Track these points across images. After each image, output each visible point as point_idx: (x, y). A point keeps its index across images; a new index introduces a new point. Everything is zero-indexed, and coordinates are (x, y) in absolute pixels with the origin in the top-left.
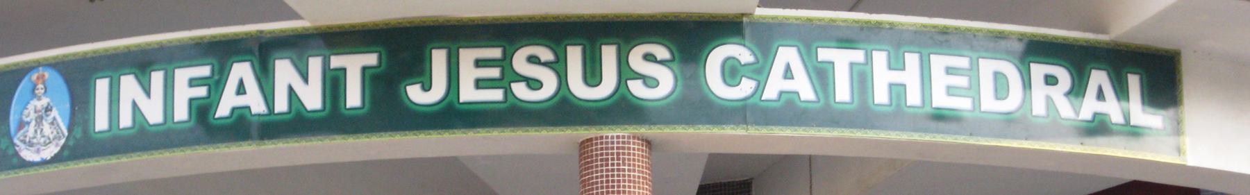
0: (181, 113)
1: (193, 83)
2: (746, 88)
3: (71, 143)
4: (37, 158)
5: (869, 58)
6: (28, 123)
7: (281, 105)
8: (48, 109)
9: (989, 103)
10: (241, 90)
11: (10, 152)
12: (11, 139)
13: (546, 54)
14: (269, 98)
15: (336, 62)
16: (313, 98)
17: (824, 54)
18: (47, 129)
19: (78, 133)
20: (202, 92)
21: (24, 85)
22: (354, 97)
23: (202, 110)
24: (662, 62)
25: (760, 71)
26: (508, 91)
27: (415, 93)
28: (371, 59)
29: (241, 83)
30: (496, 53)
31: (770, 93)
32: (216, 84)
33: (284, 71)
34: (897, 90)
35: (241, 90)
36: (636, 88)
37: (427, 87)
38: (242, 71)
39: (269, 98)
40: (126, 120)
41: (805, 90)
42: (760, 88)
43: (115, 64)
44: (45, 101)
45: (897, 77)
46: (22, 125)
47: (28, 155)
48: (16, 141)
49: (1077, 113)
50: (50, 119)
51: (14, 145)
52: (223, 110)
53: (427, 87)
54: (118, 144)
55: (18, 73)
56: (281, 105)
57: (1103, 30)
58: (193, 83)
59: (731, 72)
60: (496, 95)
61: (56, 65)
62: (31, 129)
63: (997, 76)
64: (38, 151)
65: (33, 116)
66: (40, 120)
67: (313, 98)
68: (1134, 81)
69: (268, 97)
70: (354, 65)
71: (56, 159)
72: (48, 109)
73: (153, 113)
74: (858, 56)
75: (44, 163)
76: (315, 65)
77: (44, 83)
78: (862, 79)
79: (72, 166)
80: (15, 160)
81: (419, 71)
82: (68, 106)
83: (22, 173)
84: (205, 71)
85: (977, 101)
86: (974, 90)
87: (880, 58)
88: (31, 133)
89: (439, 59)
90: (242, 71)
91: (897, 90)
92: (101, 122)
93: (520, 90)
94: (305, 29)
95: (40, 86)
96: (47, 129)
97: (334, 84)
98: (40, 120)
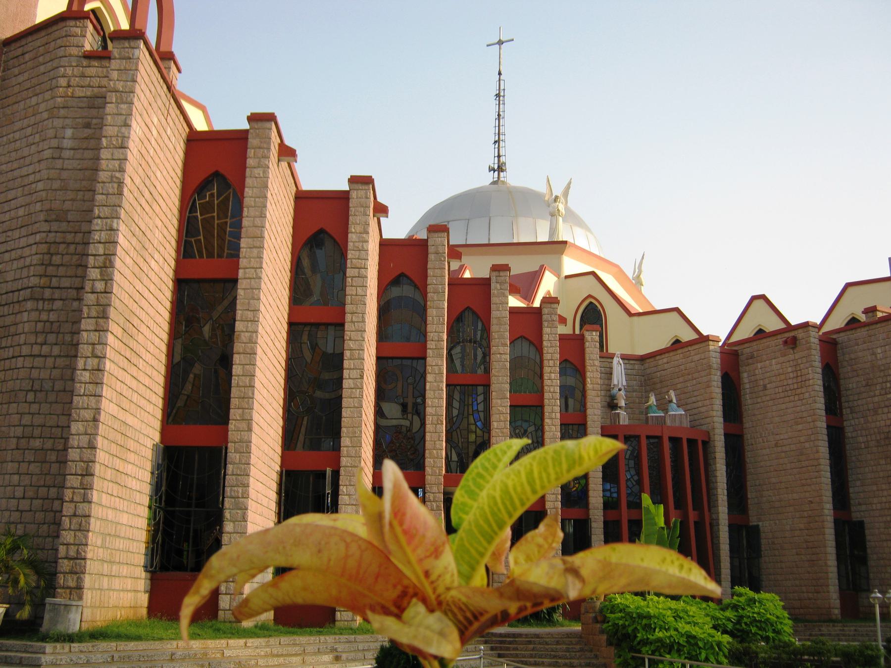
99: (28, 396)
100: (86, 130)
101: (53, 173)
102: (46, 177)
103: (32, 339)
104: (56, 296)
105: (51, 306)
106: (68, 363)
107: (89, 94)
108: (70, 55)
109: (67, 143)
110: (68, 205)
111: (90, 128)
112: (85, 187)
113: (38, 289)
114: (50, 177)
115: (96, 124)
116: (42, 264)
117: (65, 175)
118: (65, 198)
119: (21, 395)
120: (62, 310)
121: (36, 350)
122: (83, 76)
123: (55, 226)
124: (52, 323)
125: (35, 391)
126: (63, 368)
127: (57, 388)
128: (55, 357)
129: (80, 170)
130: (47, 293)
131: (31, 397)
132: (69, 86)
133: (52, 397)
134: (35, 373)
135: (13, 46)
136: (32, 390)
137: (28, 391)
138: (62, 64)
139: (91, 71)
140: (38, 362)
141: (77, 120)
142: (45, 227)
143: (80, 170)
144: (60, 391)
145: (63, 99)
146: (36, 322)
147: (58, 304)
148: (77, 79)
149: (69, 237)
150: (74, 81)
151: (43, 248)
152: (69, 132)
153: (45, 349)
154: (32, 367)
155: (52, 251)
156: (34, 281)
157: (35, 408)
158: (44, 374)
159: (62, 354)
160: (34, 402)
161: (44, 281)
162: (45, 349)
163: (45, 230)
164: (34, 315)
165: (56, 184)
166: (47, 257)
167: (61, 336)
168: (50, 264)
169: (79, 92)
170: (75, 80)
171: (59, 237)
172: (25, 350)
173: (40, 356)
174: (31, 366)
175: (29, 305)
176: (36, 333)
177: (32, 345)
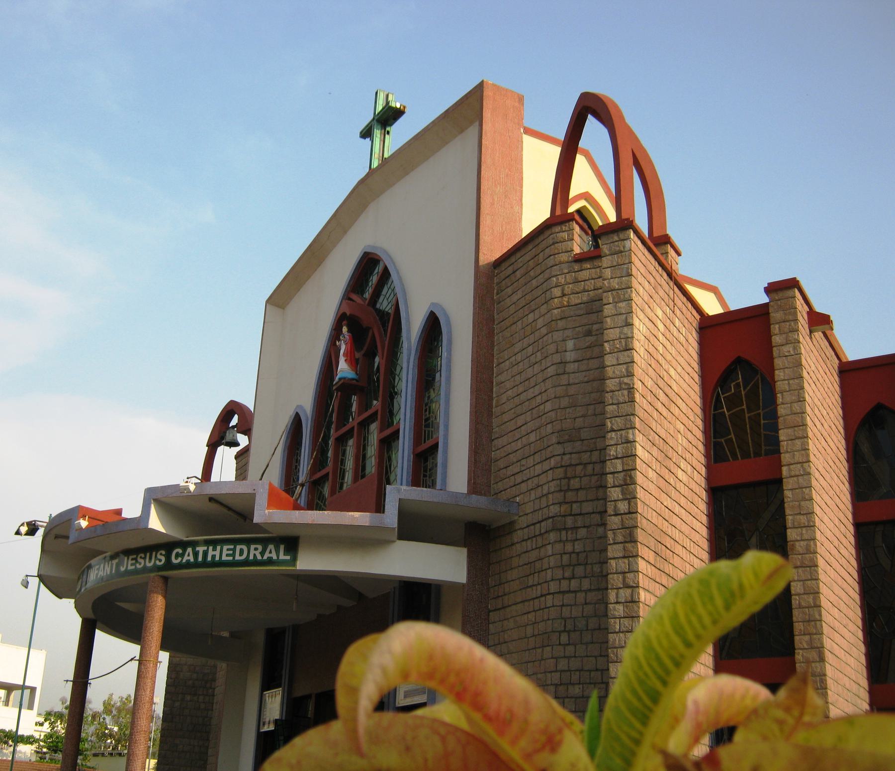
2: (180, 559)
5: (208, 548)
9: (238, 557)
25: (183, 555)
31: (184, 561)
34: (214, 556)
42: (182, 560)
45: (214, 553)
49: (263, 558)
59: (177, 555)
68: (282, 547)
74: (205, 548)
78: (205, 554)
85: (234, 557)
86: (233, 555)
87: (211, 548)
91: (214, 556)
99: (562, 638)
100: (588, 339)
101: (560, 391)
102: (553, 396)
103: (559, 573)
104: (579, 524)
105: (574, 535)
106: (600, 597)
107: (585, 299)
108: (561, 263)
109: (570, 356)
110: (579, 423)
111: (592, 336)
113: (560, 518)
114: (557, 396)
116: (561, 491)
117: (572, 390)
118: (575, 416)
121: (565, 585)
122: (576, 281)
123: (569, 447)
124: (578, 554)
125: (569, 632)
126: (595, 604)
127: (591, 626)
128: (586, 591)
129: (587, 382)
130: (569, 521)
131: (564, 638)
132: (564, 295)
133: (587, 637)
134: (566, 612)
135: (503, 266)
136: (564, 631)
137: (560, 632)
138: (554, 273)
139: (585, 274)
140: (569, 598)
141: (577, 329)
142: (559, 449)
143: (587, 382)
144: (595, 629)
145: (559, 310)
146: (561, 554)
147: (582, 532)
148: (571, 286)
149: (585, 457)
150: (567, 289)
151: (560, 472)
153: (574, 584)
154: (563, 605)
155: (569, 475)
156: (554, 510)
157: (570, 650)
158: (576, 612)
159: (593, 587)
160: (569, 644)
161: (564, 508)
162: (574, 584)
163: (559, 453)
164: (559, 547)
165: (565, 402)
166: (564, 482)
167: (589, 567)
168: (569, 490)
169: (575, 299)
170: (568, 287)
171: (575, 459)
172: (553, 587)
173: (569, 592)
174: (561, 603)
175: (552, 536)
176: (563, 567)
177: (560, 580)
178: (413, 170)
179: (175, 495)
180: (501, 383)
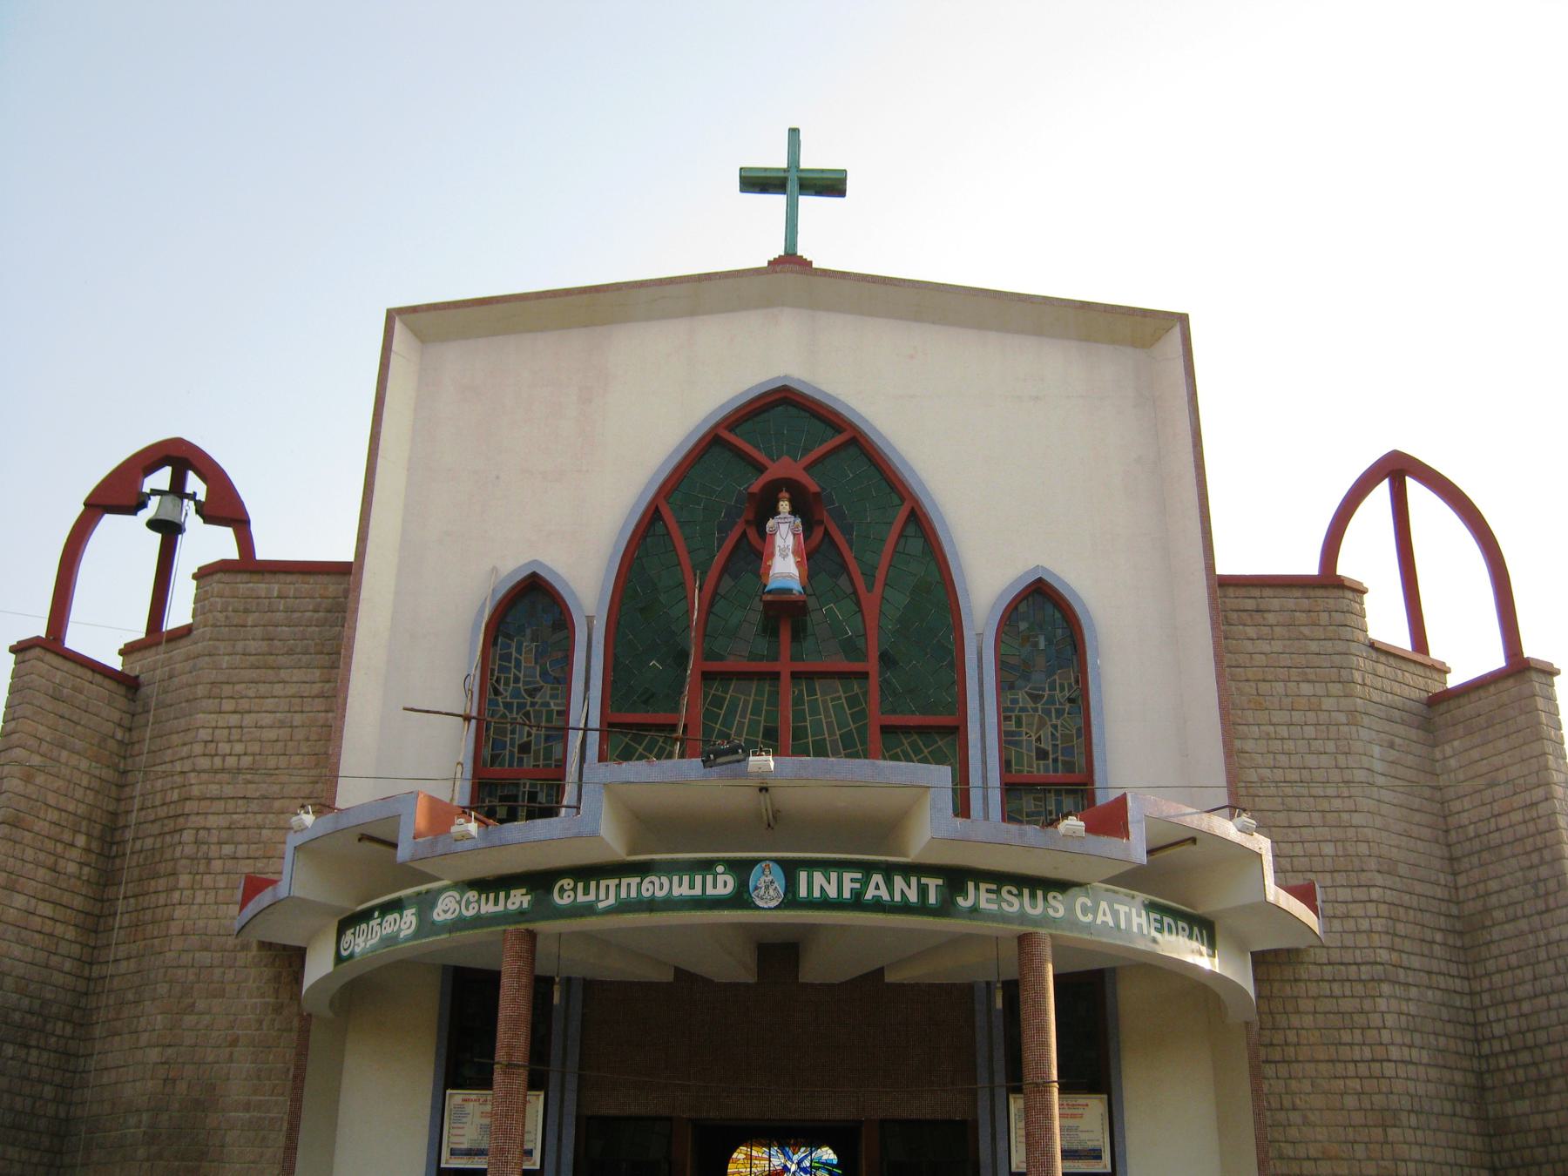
0: (847, 895)
1: (853, 880)
3: (785, 901)
4: (766, 906)
5: (1130, 910)
6: (761, 888)
7: (897, 898)
8: (772, 882)
10: (877, 887)
11: (750, 901)
12: (750, 894)
13: (1015, 891)
14: (891, 893)
15: (923, 880)
16: (913, 897)
17: (1116, 906)
18: (772, 892)
19: (790, 896)
20: (857, 885)
21: (757, 867)
22: (932, 899)
23: (858, 895)
24: (1015, 895)
26: (1000, 906)
27: (960, 900)
28: (940, 882)
29: (877, 883)
30: (994, 887)
31: (1099, 921)
32: (865, 883)
33: (898, 881)
35: (877, 887)
36: (1051, 912)
37: (966, 898)
38: (877, 878)
39: (892, 895)
40: (817, 894)
41: (1109, 920)
42: (1095, 918)
43: (812, 865)
44: (770, 878)
46: (756, 888)
47: (760, 903)
48: (753, 895)
50: (773, 887)
51: (752, 897)
52: (870, 894)
53: (966, 898)
54: (810, 904)
55: (756, 861)
56: (897, 898)
57: (1195, 910)
58: (853, 880)
59: (1085, 911)
60: (994, 907)
61: (778, 861)
62: (762, 893)
63: (1168, 924)
64: (766, 902)
65: (763, 884)
66: (767, 888)
67: (913, 897)
69: (891, 893)
70: (933, 883)
71: (776, 908)
72: (772, 882)
73: (832, 892)
75: (770, 909)
76: (914, 880)
77: (769, 868)
79: (787, 913)
80: (753, 905)
81: (963, 891)
82: (783, 882)
83: (757, 912)
84: (859, 876)
88: (762, 893)
89: (971, 885)
90: (877, 878)
92: (803, 893)
93: (1004, 906)
94: (908, 863)
95: (767, 870)
96: (772, 892)
97: (923, 891)
98: (767, 888)
99: (1411, 1119)
103: (1398, 1038)
108: (1358, 641)
109: (1378, 766)
110: (1395, 853)
112: (1405, 831)
113: (1390, 967)
115: (1400, 745)
117: (1385, 809)
119: (1404, 1116)
120: (1419, 1001)
135: (1231, 592)
138: (1353, 651)
139: (1381, 669)
142: (1379, 880)
146: (1399, 1014)
148: (1370, 676)
150: (1369, 679)
152: (1376, 750)
156: (1384, 955)
164: (1394, 1004)
165: (1379, 822)
169: (1376, 696)
172: (1395, 1053)
175: (1386, 988)
178: (933, 323)
179: (1175, 820)
180: (1242, 752)
